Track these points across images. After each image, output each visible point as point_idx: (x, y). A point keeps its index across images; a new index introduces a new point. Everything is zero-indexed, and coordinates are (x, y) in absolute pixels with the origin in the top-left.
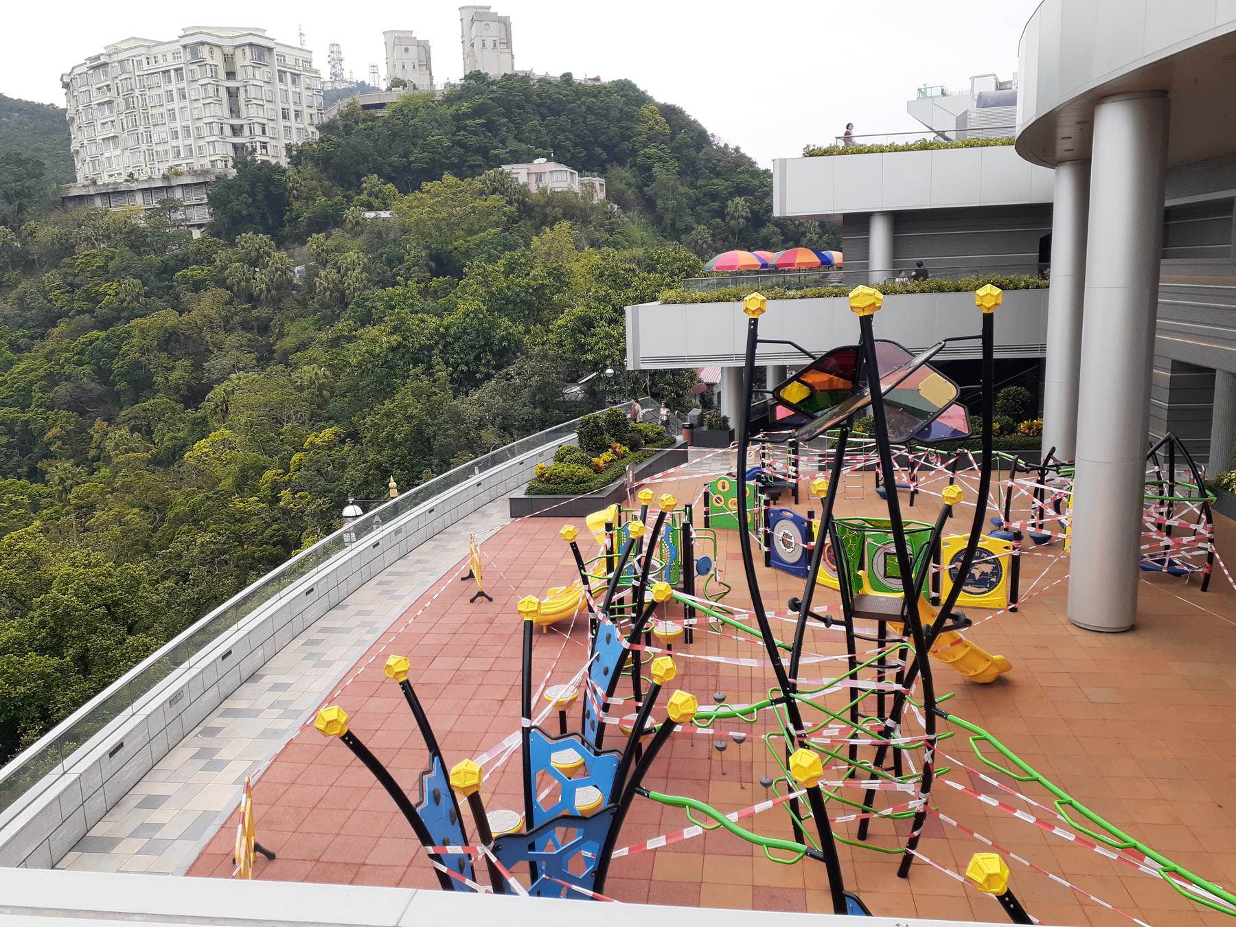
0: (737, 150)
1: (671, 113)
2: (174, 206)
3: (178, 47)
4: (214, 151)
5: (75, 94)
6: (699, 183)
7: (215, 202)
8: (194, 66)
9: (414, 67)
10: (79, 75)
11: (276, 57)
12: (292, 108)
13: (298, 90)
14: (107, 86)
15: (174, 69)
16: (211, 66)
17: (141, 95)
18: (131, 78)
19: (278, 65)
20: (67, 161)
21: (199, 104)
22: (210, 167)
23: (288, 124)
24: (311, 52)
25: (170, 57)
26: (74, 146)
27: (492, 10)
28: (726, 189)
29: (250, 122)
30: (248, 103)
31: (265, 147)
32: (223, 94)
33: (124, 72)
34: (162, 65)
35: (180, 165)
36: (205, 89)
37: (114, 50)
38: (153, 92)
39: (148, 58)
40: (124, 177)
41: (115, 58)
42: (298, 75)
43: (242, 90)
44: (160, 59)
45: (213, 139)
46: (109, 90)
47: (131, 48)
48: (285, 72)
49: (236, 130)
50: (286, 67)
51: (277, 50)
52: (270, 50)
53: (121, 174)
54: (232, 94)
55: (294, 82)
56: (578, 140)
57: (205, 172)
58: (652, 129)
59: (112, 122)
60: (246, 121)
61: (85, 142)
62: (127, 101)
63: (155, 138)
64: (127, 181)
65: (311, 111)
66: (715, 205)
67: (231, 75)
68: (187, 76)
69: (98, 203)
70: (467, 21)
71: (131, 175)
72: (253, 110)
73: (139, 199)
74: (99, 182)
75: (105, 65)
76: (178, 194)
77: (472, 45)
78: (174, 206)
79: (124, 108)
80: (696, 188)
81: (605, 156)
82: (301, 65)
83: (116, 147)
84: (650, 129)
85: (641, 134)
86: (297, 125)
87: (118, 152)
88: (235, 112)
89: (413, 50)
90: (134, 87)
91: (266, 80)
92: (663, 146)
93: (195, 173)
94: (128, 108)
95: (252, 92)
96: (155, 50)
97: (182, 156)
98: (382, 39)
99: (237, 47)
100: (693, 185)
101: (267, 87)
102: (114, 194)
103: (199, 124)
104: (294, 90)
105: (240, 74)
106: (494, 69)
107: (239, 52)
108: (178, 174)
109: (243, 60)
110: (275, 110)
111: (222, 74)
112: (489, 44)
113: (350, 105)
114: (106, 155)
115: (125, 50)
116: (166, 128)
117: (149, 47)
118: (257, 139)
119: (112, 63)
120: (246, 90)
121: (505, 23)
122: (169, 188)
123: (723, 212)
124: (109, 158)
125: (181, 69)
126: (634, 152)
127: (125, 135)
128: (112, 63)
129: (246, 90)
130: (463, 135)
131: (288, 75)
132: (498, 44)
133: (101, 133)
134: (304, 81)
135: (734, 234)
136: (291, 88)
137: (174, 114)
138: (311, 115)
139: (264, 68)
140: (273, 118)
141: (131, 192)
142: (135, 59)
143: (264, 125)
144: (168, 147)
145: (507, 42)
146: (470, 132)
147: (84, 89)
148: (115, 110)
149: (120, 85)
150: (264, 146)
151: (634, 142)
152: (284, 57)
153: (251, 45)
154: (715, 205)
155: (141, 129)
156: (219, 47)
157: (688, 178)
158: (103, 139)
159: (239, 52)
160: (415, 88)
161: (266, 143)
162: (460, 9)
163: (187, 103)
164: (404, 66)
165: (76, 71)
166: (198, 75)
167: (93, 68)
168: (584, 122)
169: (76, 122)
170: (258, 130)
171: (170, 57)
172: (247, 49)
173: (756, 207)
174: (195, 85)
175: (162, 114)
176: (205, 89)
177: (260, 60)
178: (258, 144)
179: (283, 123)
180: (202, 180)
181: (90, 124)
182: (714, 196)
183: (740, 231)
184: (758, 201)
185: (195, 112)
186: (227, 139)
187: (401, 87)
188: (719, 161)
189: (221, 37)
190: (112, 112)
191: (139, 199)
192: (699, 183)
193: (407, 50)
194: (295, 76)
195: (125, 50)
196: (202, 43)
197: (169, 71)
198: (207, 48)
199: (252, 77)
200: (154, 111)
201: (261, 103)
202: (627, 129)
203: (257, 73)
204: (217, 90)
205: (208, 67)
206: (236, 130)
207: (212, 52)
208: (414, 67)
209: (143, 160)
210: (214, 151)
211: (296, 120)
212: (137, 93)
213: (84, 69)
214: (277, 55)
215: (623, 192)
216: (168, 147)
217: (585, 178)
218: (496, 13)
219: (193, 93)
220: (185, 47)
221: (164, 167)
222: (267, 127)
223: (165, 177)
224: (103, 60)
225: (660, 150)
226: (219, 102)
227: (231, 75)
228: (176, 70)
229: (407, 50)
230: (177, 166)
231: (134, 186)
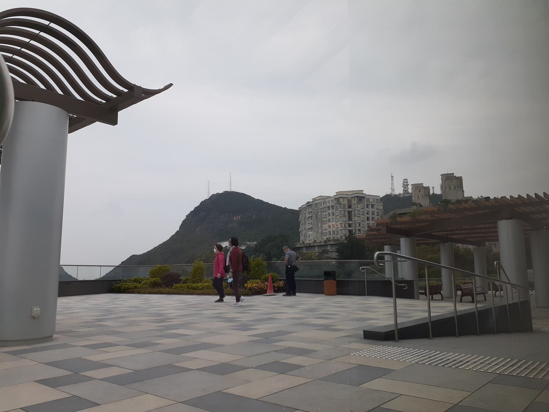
2: (326, 252)
3: (333, 199)
4: (342, 232)
5: (302, 213)
7: (338, 251)
8: (338, 205)
9: (423, 197)
10: (303, 208)
11: (366, 200)
12: (370, 216)
13: (374, 210)
14: (311, 211)
15: (331, 206)
17: (321, 214)
18: (318, 209)
19: (367, 202)
20: (298, 234)
21: (338, 217)
22: (340, 238)
23: (369, 222)
25: (330, 202)
26: (300, 230)
27: (454, 175)
30: (355, 215)
31: (360, 231)
32: (347, 213)
33: (316, 207)
34: (328, 205)
35: (331, 237)
36: (341, 212)
37: (314, 200)
38: (324, 213)
40: (313, 241)
41: (314, 203)
42: (374, 205)
43: (353, 212)
44: (328, 203)
45: (342, 228)
46: (311, 213)
47: (319, 200)
48: (369, 204)
49: (350, 225)
50: (369, 203)
51: (367, 197)
52: (364, 197)
53: (312, 240)
54: (350, 213)
55: (372, 207)
57: (338, 240)
59: (311, 223)
60: (354, 222)
61: (303, 229)
62: (316, 216)
63: (323, 228)
64: (313, 242)
67: (350, 207)
68: (335, 208)
69: (304, 251)
70: (444, 179)
71: (315, 240)
72: (356, 218)
73: (317, 249)
74: (305, 243)
75: (311, 205)
76: (329, 248)
77: (446, 188)
78: (326, 252)
79: (315, 218)
82: (375, 201)
83: (312, 231)
86: (372, 222)
87: (312, 233)
88: (350, 219)
89: (422, 191)
90: (319, 212)
91: (362, 207)
93: (334, 240)
94: (316, 219)
95: (356, 212)
96: (326, 200)
97: (331, 234)
99: (352, 197)
101: (362, 210)
102: (309, 247)
103: (338, 223)
105: (353, 206)
106: (453, 197)
107: (353, 198)
108: (329, 241)
109: (354, 202)
111: (347, 207)
112: (452, 188)
113: (393, 214)
114: (309, 233)
115: (317, 200)
116: (327, 225)
117: (324, 199)
118: (357, 228)
119: (313, 204)
120: (354, 212)
121: (460, 179)
122: (326, 245)
124: (309, 234)
125: (333, 206)
127: (315, 227)
128: (313, 204)
129: (354, 212)
131: (370, 205)
132: (456, 187)
133: (308, 226)
136: (371, 210)
137: (330, 220)
138: (378, 218)
141: (314, 246)
143: (360, 223)
144: (327, 231)
147: (304, 212)
148: (313, 219)
149: (315, 211)
150: (360, 230)
152: (369, 199)
153: (357, 197)
155: (320, 225)
158: (308, 228)
159: (353, 199)
160: (421, 206)
161: (360, 229)
162: (441, 175)
163: (334, 217)
164: (418, 197)
165: (303, 207)
166: (339, 208)
167: (307, 206)
169: (302, 222)
170: (358, 225)
171: (330, 202)
172: (356, 198)
174: (337, 211)
175: (326, 220)
176: (341, 212)
177: (360, 201)
178: (357, 230)
179: (367, 222)
180: (337, 243)
181: (305, 223)
185: (337, 220)
186: (347, 228)
187: (415, 206)
190: (311, 220)
191: (317, 249)
193: (420, 191)
195: (317, 200)
196: (341, 197)
198: (342, 199)
199: (358, 207)
200: (324, 219)
203: (359, 205)
204: (345, 212)
206: (350, 225)
207: (344, 200)
208: (423, 197)
209: (319, 235)
210: (342, 232)
211: (372, 220)
212: (320, 214)
213: (305, 206)
214: (367, 199)
216: (327, 231)
219: (337, 213)
220: (335, 199)
221: (325, 238)
222: (361, 223)
223: (325, 241)
224: (310, 203)
226: (345, 216)
227: (350, 207)
228: (332, 206)
229: (420, 191)
230: (329, 237)
231: (315, 244)
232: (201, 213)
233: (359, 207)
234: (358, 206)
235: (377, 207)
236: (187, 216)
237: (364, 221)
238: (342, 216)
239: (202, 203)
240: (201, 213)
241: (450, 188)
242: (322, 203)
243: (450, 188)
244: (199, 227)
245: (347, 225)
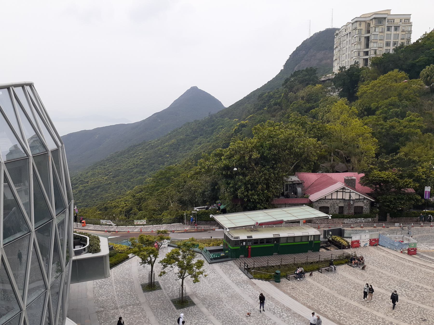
13: (398, 33)
16: (359, 29)
24: (411, 15)
29: (359, 51)
39: (345, 30)
42: (399, 26)
48: (391, 26)
49: (367, 53)
51: (389, 17)
54: (368, 39)
65: (403, 41)
82: (403, 21)
88: (367, 46)
91: (381, 31)
99: (371, 20)
101: (381, 34)
104: (395, 33)
110: (382, 44)
111: (363, 32)
134: (401, 29)
139: (381, 27)
140: (381, 46)
142: (342, 31)
143: (376, 50)
152: (394, 20)
153: (375, 18)
156: (364, 21)
170: (372, 52)
172: (374, 20)
186: (361, 58)
189: (366, 17)
194: (396, 28)
197: (348, 34)
198: (358, 23)
201: (376, 41)
205: (357, 30)
207: (360, 25)
220: (352, 24)
227: (369, 32)
232: (301, 51)
233: (377, 31)
234: (375, 31)
235: (403, 28)
236: (290, 56)
237: (382, 47)
238: (356, 43)
239: (304, 43)
240: (301, 51)
242: (344, 30)
244: (298, 66)
245: (362, 54)
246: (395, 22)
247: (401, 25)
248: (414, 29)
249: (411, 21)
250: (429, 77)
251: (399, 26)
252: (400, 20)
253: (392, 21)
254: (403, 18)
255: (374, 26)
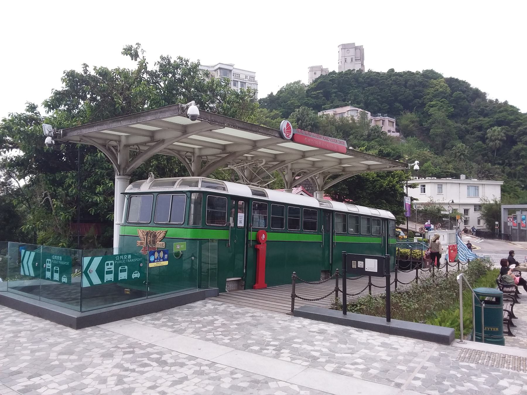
0: (506, 103)
1: (453, 82)
6: (469, 120)
24: (255, 73)
28: (488, 123)
42: (245, 83)
48: (238, 81)
52: (231, 71)
56: (384, 100)
58: (437, 90)
66: (478, 133)
80: (467, 124)
81: (402, 107)
82: (248, 78)
84: (435, 91)
85: (429, 94)
92: (444, 99)
98: (308, 70)
99: (215, 71)
100: (465, 122)
107: (216, 72)
123: (484, 137)
126: (423, 105)
130: (308, 99)
131: (239, 83)
135: (493, 152)
145: (361, 59)
146: (312, 97)
151: (424, 99)
153: (220, 68)
154: (478, 133)
157: (462, 119)
168: (389, 89)
172: (218, 71)
173: (510, 133)
182: (480, 128)
183: (498, 150)
184: (513, 129)
188: (486, 107)
192: (469, 120)
193: (315, 74)
202: (420, 92)
215: (408, 126)
217: (378, 117)
218: (354, 44)
225: (442, 102)
241: (346, 61)
243: (346, 61)
246: (240, 77)
247: (247, 82)
248: (260, 88)
249: (256, 79)
250: (300, 121)
251: (245, 83)
252: (246, 76)
253: (237, 76)
254: (248, 75)
255: (220, 78)
